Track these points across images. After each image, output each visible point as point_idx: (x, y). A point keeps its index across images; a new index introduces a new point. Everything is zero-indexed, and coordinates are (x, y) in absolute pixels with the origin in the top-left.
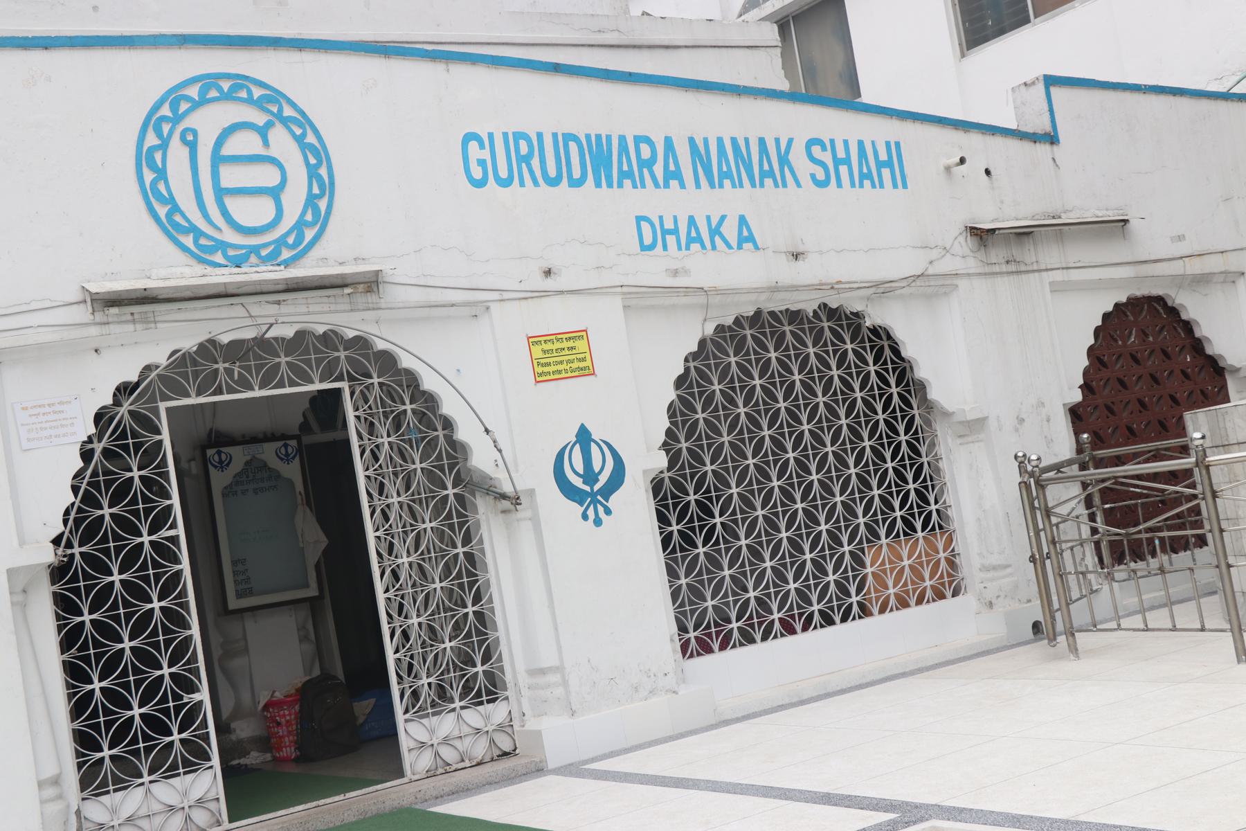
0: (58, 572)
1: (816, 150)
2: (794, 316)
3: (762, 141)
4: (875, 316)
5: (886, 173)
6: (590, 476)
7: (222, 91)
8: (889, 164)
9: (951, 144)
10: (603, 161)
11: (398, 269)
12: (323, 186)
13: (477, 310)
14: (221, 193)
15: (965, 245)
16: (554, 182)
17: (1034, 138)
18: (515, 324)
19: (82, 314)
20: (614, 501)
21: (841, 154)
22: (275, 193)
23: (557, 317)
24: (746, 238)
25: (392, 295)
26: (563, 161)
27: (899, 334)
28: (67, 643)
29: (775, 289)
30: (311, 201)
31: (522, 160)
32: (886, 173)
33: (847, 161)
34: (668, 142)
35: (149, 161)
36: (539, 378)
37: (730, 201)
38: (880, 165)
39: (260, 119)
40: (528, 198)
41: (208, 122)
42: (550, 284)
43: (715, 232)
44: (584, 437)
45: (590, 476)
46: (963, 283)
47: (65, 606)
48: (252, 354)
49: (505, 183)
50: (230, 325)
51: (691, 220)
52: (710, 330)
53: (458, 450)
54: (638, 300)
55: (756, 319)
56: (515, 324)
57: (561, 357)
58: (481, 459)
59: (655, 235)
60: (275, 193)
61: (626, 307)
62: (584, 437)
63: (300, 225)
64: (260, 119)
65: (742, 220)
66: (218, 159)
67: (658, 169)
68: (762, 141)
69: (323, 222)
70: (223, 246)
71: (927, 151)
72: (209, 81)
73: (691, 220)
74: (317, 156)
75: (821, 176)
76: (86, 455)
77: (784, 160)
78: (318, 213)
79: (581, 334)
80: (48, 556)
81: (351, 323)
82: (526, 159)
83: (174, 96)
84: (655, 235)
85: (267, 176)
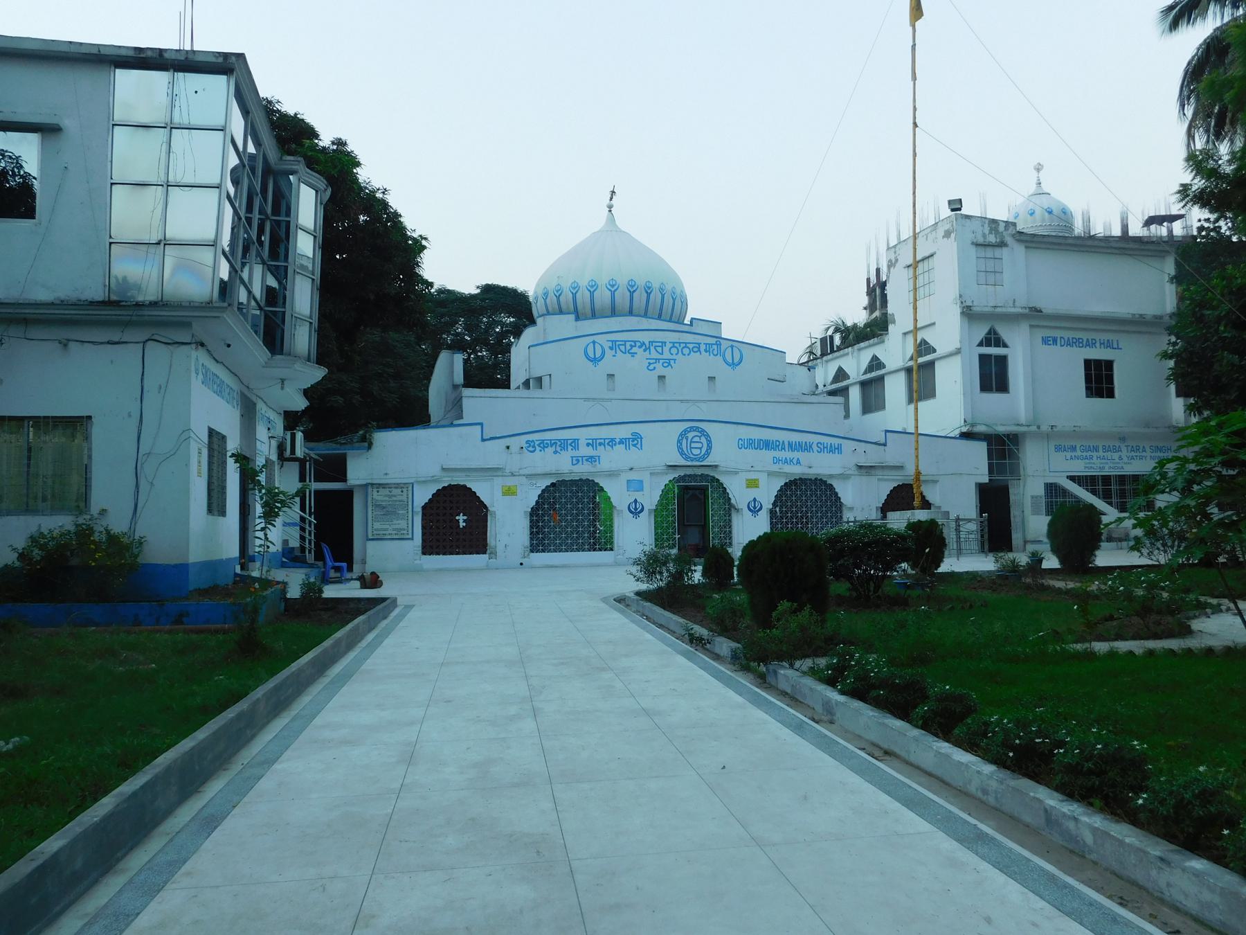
4: (829, 482)
7: (695, 429)
10: (767, 445)
11: (722, 464)
12: (710, 448)
13: (736, 473)
18: (743, 477)
23: (752, 476)
24: (798, 462)
31: (751, 444)
35: (679, 442)
40: (751, 454)
41: (690, 435)
50: (689, 472)
56: (743, 477)
57: (753, 484)
58: (733, 501)
59: (777, 461)
71: (848, 446)
74: (709, 442)
78: (708, 453)
83: (685, 430)
84: (777, 461)
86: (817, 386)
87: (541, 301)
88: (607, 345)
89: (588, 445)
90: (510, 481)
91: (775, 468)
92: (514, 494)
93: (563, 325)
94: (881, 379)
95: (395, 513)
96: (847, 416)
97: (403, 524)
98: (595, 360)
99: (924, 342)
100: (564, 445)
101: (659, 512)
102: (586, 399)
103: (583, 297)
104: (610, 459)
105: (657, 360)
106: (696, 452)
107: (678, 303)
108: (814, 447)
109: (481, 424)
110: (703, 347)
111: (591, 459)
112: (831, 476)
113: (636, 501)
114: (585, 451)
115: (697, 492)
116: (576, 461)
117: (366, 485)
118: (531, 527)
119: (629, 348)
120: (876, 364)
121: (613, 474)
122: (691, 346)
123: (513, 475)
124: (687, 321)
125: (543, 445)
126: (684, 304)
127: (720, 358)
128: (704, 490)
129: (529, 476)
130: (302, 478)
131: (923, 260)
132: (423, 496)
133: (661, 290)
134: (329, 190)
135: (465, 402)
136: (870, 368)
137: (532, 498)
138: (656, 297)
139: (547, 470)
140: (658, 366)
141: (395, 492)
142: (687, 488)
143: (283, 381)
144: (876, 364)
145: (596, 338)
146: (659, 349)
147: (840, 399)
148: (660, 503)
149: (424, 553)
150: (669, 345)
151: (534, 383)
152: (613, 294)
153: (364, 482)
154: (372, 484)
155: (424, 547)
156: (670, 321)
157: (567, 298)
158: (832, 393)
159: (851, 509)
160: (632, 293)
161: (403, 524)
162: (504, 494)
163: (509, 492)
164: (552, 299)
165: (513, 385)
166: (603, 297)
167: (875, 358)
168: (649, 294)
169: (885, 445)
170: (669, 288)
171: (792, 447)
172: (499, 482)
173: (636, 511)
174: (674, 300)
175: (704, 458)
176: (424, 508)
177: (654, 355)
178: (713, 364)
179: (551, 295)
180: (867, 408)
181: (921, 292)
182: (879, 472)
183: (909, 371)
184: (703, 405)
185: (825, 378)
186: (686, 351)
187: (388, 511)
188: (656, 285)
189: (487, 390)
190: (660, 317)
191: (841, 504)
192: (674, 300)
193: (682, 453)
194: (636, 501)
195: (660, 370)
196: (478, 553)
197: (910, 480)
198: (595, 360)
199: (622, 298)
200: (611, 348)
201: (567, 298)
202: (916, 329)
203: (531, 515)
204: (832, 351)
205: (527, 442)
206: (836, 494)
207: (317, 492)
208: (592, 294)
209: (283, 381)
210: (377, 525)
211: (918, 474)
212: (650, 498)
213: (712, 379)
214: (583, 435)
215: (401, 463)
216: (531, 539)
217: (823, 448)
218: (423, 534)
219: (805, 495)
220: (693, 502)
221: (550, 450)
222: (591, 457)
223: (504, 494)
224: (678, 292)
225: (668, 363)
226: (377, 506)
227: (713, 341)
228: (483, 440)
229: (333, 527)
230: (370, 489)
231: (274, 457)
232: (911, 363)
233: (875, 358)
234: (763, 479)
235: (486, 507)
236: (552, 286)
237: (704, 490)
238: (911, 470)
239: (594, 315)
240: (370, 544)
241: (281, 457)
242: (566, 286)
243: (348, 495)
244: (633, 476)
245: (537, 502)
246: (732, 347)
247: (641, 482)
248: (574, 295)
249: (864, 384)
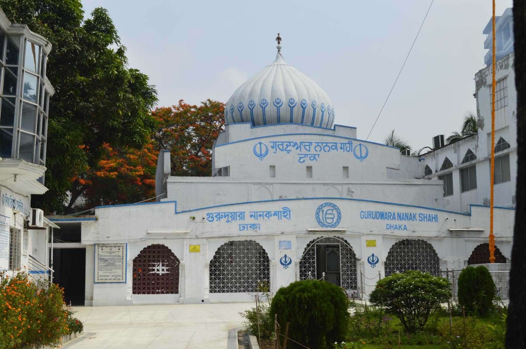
0: (300, 263)
1: (421, 215)
2: (415, 241)
3: (411, 214)
4: (428, 242)
5: (434, 219)
6: (373, 261)
7: (328, 206)
8: (435, 218)
9: (446, 215)
10: (382, 216)
12: (339, 218)
14: (326, 218)
15: (448, 232)
16: (374, 218)
17: (466, 215)
18: (364, 239)
19: (307, 232)
20: (376, 265)
21: (425, 216)
22: (333, 218)
23: (371, 238)
24: (405, 228)
25: (347, 233)
26: (376, 215)
27: (433, 245)
28: (300, 272)
29: (409, 237)
30: (338, 220)
31: (370, 215)
32: (434, 219)
33: (426, 217)
34: (394, 214)
35: (317, 214)
36: (367, 246)
37: (403, 223)
38: (433, 218)
39: (332, 209)
40: (369, 221)
41: (325, 209)
42: (371, 233)
43: (400, 227)
44: (373, 255)
45: (373, 261)
46: (446, 238)
47: (301, 267)
48: (328, 239)
49: (366, 218)
50: (325, 236)
51: (396, 225)
52: (397, 241)
53: (354, 255)
54: (385, 237)
55: (407, 240)
56: (364, 239)
57: (371, 244)
60: (333, 218)
61: (383, 237)
62: (373, 255)
63: (336, 223)
64: (332, 209)
65: (405, 226)
66: (326, 214)
67: (392, 217)
68: (411, 214)
69: (339, 223)
70: (325, 225)
71: (442, 216)
72: (326, 204)
73: (396, 225)
74: (339, 214)
75: (421, 219)
76: (306, 249)
77: (414, 217)
78: (338, 221)
79: (375, 241)
80: (299, 261)
81: (341, 236)
82: (370, 215)
83: (321, 206)
85: (332, 216)
86: (428, 171)
87: (229, 115)
88: (269, 145)
89: (251, 216)
90: (195, 242)
91: (388, 232)
92: (198, 251)
93: (237, 131)
94: (473, 167)
95: (113, 264)
96: (448, 191)
97: (119, 272)
98: (261, 156)
99: (502, 140)
100: (233, 216)
101: (304, 264)
102: (254, 184)
103: (257, 111)
104: (267, 226)
105: (306, 155)
106: (329, 221)
107: (326, 115)
108: (417, 217)
109: (175, 202)
110: (339, 146)
111: (253, 226)
112: (430, 238)
113: (285, 256)
114: (248, 220)
115: (335, 249)
116: (243, 227)
117: (95, 245)
118: (211, 275)
119: (285, 147)
120: (470, 156)
121: (270, 237)
122: (330, 145)
123: (197, 238)
124: (333, 128)
125: (219, 216)
126: (331, 115)
127: (351, 153)
128: (338, 247)
129: (207, 238)
130: (50, 241)
131: (499, 81)
132: (133, 253)
133: (313, 105)
134: (50, 46)
135: (169, 186)
136: (466, 159)
137: (210, 256)
138: (309, 110)
139: (222, 234)
140: (307, 159)
141: (115, 249)
142: (328, 246)
143: (15, 175)
144: (470, 156)
145: (262, 140)
146: (307, 148)
147: (441, 182)
148: (304, 258)
149: (134, 293)
150: (314, 145)
151: (224, 171)
152: (278, 109)
153: (93, 243)
154: (98, 245)
155: (134, 288)
156: (320, 127)
157: (246, 111)
158: (440, 177)
159: (446, 262)
160: (292, 108)
161: (119, 272)
162: (191, 251)
163: (194, 250)
164: (236, 112)
165: (213, 174)
166: (271, 111)
167: (469, 152)
168: (304, 109)
169: (469, 215)
170: (318, 104)
171: (400, 217)
172: (186, 242)
173: (285, 263)
174: (323, 112)
175: (335, 226)
176: (135, 261)
177: (304, 152)
178: (346, 158)
179: (236, 110)
180: (464, 188)
181: (498, 105)
182: (466, 235)
183: (490, 160)
184: (340, 188)
185: (437, 165)
186: (327, 148)
187: (108, 263)
188: (308, 102)
189: (185, 177)
190: (312, 124)
191: (438, 259)
192: (323, 112)
193: (319, 222)
194: (285, 256)
195: (308, 162)
196: (172, 293)
197: (487, 241)
198: (261, 156)
199: (284, 111)
200: (273, 147)
201: (246, 111)
202: (493, 132)
203: (211, 266)
204: (443, 146)
205: (207, 215)
206: (434, 251)
207: (55, 250)
208: (264, 109)
209: (15, 175)
210: (101, 273)
211: (492, 236)
212: (296, 254)
213: (346, 168)
214: (247, 209)
215: (116, 230)
216: (211, 283)
217: (423, 218)
218: (134, 279)
219: (409, 253)
220: (328, 257)
221: (224, 220)
222: (254, 225)
223: (191, 251)
224: (326, 106)
225: (314, 157)
226: (102, 260)
227: (346, 141)
228: (176, 213)
229: (70, 274)
230: (97, 247)
231: (20, 226)
232: (490, 157)
233: (469, 152)
234: (379, 241)
235: (178, 260)
236: (236, 105)
237: (338, 247)
238: (487, 234)
239: (265, 123)
240: (96, 285)
241: (26, 226)
242: (246, 103)
243: (83, 251)
244: (283, 238)
245: (215, 257)
246: (360, 145)
247: (290, 242)
248: (251, 110)
249: (463, 171)
